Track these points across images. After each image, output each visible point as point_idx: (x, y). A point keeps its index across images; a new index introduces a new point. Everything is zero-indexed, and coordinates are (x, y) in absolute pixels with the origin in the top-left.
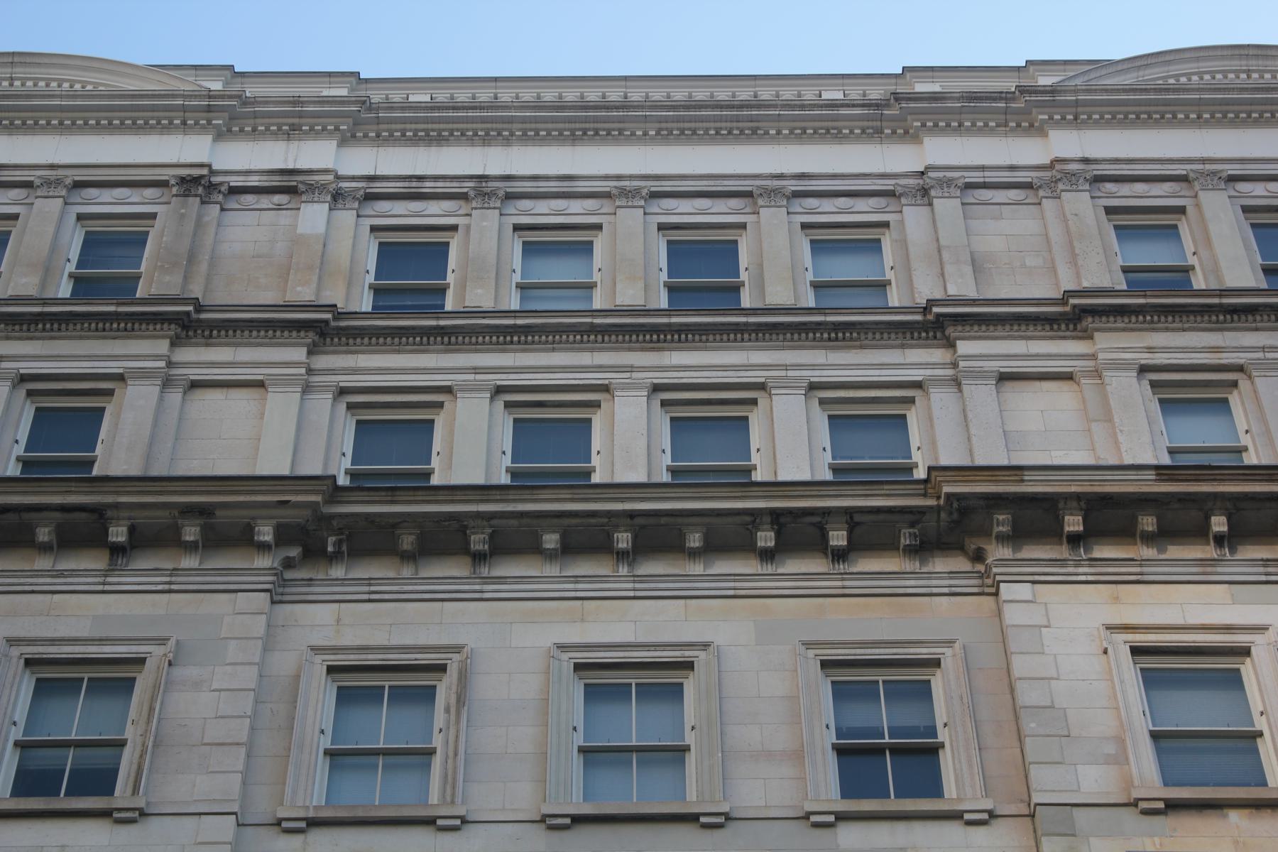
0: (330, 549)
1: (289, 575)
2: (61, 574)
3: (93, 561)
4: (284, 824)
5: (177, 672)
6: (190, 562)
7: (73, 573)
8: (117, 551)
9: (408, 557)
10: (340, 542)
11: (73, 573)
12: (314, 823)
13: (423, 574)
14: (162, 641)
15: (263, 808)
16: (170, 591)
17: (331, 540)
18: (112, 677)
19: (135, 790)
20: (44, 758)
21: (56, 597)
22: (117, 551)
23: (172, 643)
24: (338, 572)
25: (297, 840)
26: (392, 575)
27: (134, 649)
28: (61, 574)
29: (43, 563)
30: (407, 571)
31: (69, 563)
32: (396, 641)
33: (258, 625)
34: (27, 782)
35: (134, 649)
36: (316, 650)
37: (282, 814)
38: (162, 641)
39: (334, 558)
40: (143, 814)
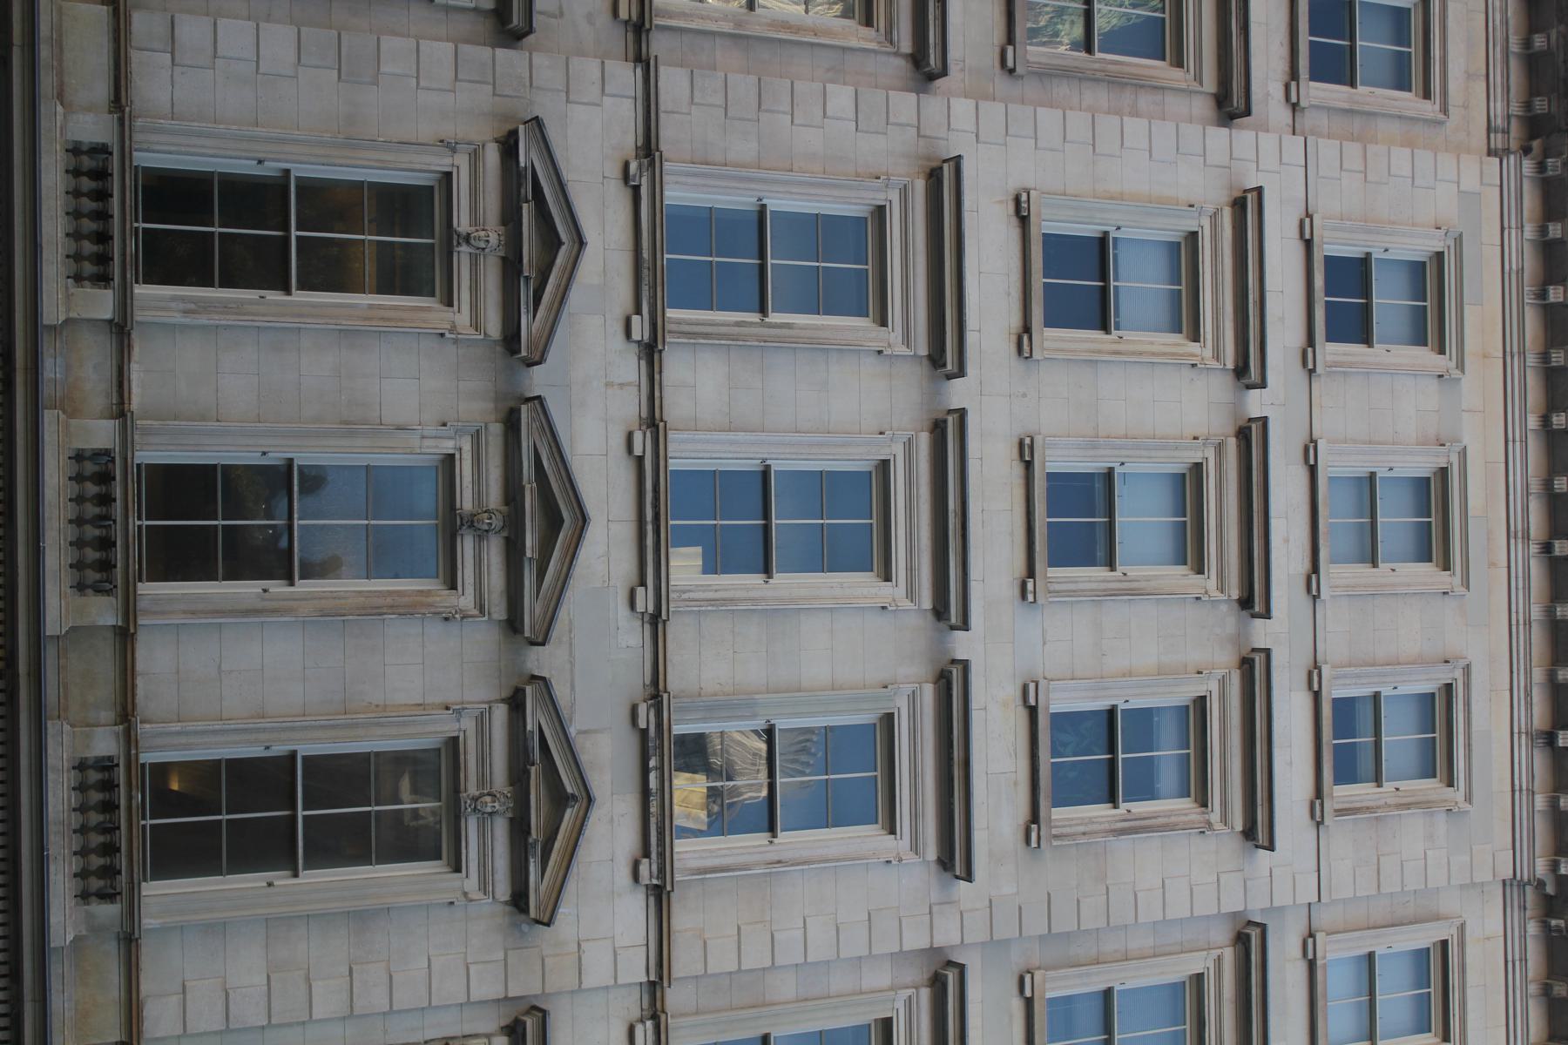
0: (1554, 922)
1: (1529, 889)
2: (1528, 694)
3: (1540, 715)
4: (1310, 941)
5: (1441, 818)
6: (1540, 802)
7: (1529, 704)
8: (1550, 738)
9: (1546, 991)
10: (1558, 929)
11: (1529, 704)
12: (1312, 965)
13: (1531, 1003)
14: (1469, 798)
15: (1323, 918)
16: (1513, 791)
17: (1562, 923)
18: (1438, 759)
19: (1340, 812)
20: (1365, 716)
21: (1508, 693)
22: (1550, 738)
23: (1467, 807)
24: (1533, 928)
25: (1298, 952)
26: (1530, 974)
27: (1462, 776)
28: (1528, 694)
29: (1538, 675)
30: (1533, 988)
31: (1538, 696)
32: (1471, 993)
33: (1484, 875)
34: (1344, 708)
35: (1462, 776)
36: (1462, 928)
37: (1320, 937)
38: (1469, 798)
39: (1546, 927)
40: (1318, 824)
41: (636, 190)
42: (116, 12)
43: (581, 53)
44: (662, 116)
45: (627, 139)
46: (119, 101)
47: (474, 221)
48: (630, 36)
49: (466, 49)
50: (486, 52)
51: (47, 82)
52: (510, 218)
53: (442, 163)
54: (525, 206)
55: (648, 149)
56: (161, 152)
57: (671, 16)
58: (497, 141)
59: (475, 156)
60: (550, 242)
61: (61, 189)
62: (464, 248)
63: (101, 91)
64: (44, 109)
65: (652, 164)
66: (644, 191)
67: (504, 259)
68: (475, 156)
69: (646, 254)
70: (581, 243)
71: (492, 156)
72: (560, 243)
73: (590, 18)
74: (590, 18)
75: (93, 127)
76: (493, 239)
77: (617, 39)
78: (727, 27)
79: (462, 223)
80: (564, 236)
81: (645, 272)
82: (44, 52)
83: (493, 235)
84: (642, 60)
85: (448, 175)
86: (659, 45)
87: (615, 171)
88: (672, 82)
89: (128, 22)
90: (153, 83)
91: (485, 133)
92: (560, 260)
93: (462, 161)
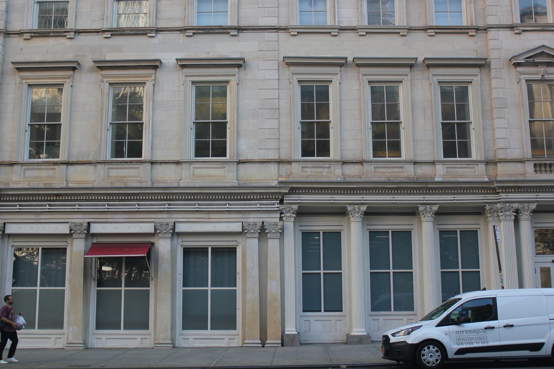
41: (523, 31)
42: (500, 162)
43: (487, 45)
44: (501, 24)
45: (508, 33)
46: (522, 161)
47: (538, 74)
48: (479, 32)
49: (493, 75)
50: (493, 71)
51: (521, 178)
52: (536, 65)
53: (523, 82)
54: (536, 61)
55: (511, 27)
56: (528, 152)
57: (472, 21)
58: (515, 68)
59: (521, 73)
60: (542, 54)
61: (541, 175)
62: (545, 76)
63: (519, 165)
64: (529, 179)
65: (516, 27)
66: (523, 29)
67: (547, 66)
68: (521, 73)
69: (540, 28)
70: (543, 46)
71: (520, 69)
72: (543, 52)
73: (476, 43)
74: (476, 43)
75: (529, 167)
76: (543, 69)
77: (481, 36)
78: (472, 5)
79: (539, 77)
80: (541, 51)
81: (545, 29)
82: (513, 178)
83: (542, 69)
84: (486, 29)
85: (526, 80)
86: (481, 24)
87: (518, 36)
88: (491, 21)
89: (502, 159)
90: (516, 154)
91: (513, 71)
92: (547, 52)
93: (523, 77)
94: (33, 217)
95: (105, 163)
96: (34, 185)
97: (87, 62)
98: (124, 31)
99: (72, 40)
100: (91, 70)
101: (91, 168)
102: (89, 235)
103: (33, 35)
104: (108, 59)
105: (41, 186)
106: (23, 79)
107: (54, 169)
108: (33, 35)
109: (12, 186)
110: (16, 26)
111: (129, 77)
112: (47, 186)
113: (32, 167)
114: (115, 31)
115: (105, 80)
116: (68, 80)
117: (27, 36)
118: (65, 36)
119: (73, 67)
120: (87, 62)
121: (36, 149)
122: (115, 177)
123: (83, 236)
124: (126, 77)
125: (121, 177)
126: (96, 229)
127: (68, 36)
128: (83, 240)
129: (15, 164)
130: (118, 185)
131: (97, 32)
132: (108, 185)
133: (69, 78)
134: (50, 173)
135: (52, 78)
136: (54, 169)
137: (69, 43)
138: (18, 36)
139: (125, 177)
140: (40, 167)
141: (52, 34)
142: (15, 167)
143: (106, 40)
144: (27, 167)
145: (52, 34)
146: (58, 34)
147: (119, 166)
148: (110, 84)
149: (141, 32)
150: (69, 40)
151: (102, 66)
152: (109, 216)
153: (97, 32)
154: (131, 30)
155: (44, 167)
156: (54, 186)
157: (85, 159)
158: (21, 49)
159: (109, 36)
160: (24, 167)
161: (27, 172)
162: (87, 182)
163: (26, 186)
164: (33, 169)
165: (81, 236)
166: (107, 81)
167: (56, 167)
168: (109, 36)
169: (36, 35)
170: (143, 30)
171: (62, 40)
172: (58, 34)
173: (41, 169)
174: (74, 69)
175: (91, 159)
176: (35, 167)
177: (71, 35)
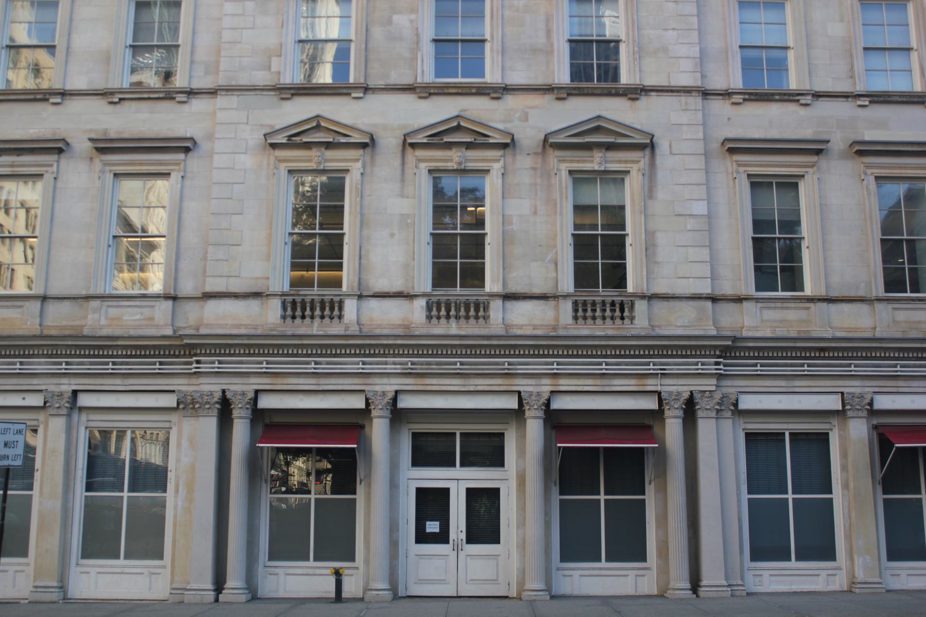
94: (782, 383)
95: (879, 300)
96: (781, 332)
97: (838, 142)
98: (889, 96)
99: (807, 108)
100: (843, 156)
101: (864, 308)
102: (873, 413)
103: (747, 97)
104: (867, 138)
105: (793, 334)
106: (739, 165)
107: (808, 308)
108: (747, 97)
109: (745, 334)
110: (717, 82)
111: (906, 168)
112: (802, 335)
113: (772, 305)
114: (876, 96)
115: (869, 171)
116: (810, 170)
117: (738, 98)
118: (798, 101)
119: (815, 149)
120: (838, 142)
121: (764, 278)
122: (905, 322)
123: (865, 414)
124: (901, 168)
125: (914, 322)
126: (883, 402)
127: (802, 102)
128: (864, 420)
129: (746, 299)
130: (913, 334)
131: (846, 96)
132: (899, 335)
133: (812, 166)
134: (802, 314)
135: (786, 166)
136: (808, 308)
137: (802, 112)
138: (721, 97)
139: (919, 322)
140: (785, 305)
141: (777, 97)
142: (745, 304)
143: (860, 110)
144: (765, 305)
145: (777, 97)
146: (786, 97)
147: (909, 306)
148: (877, 178)
149: (915, 100)
150: (802, 108)
151: (863, 150)
152: (901, 383)
153: (846, 96)
154: (900, 96)
155: (793, 305)
156: (814, 335)
157: (852, 294)
158: (729, 119)
159: (867, 103)
160: (760, 305)
161: (765, 312)
162: (856, 330)
163: (768, 333)
164: (775, 308)
165: (860, 414)
166: (872, 174)
167: (811, 305)
168: (867, 103)
169: (753, 97)
170: (920, 97)
171: (792, 107)
172: (786, 97)
173: (787, 308)
174: (818, 152)
175: (861, 293)
176: (778, 305)
177: (808, 99)
